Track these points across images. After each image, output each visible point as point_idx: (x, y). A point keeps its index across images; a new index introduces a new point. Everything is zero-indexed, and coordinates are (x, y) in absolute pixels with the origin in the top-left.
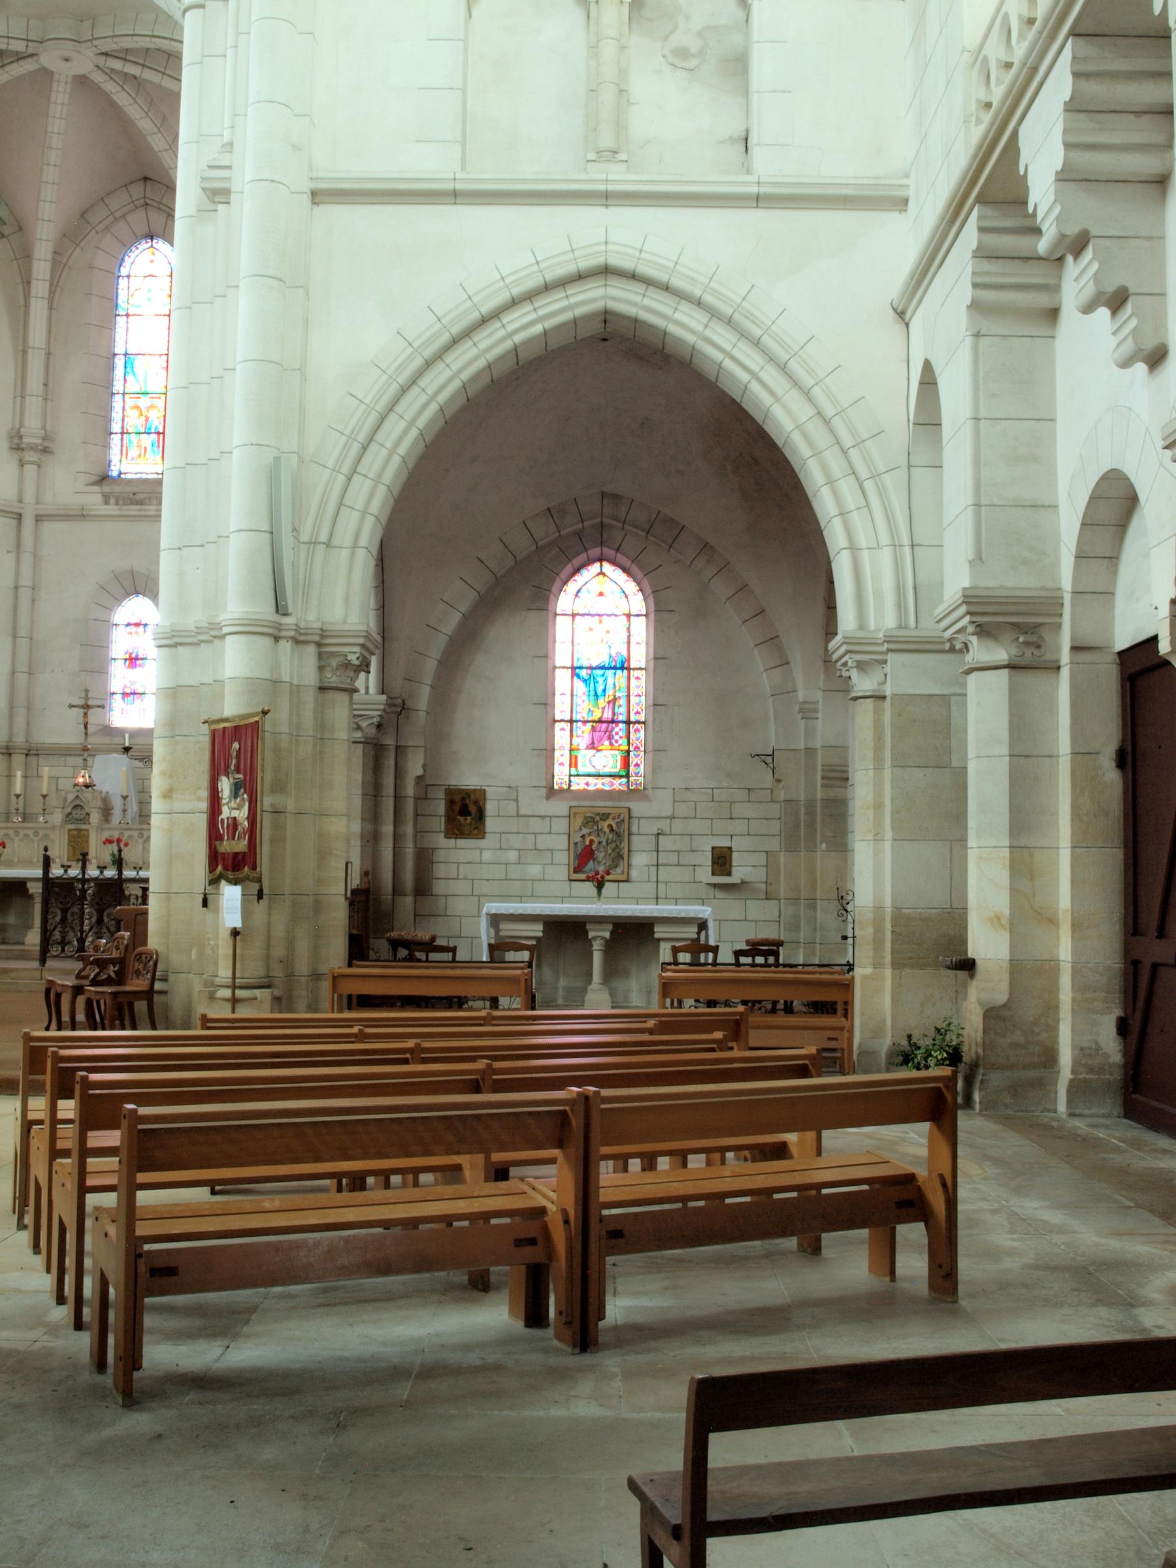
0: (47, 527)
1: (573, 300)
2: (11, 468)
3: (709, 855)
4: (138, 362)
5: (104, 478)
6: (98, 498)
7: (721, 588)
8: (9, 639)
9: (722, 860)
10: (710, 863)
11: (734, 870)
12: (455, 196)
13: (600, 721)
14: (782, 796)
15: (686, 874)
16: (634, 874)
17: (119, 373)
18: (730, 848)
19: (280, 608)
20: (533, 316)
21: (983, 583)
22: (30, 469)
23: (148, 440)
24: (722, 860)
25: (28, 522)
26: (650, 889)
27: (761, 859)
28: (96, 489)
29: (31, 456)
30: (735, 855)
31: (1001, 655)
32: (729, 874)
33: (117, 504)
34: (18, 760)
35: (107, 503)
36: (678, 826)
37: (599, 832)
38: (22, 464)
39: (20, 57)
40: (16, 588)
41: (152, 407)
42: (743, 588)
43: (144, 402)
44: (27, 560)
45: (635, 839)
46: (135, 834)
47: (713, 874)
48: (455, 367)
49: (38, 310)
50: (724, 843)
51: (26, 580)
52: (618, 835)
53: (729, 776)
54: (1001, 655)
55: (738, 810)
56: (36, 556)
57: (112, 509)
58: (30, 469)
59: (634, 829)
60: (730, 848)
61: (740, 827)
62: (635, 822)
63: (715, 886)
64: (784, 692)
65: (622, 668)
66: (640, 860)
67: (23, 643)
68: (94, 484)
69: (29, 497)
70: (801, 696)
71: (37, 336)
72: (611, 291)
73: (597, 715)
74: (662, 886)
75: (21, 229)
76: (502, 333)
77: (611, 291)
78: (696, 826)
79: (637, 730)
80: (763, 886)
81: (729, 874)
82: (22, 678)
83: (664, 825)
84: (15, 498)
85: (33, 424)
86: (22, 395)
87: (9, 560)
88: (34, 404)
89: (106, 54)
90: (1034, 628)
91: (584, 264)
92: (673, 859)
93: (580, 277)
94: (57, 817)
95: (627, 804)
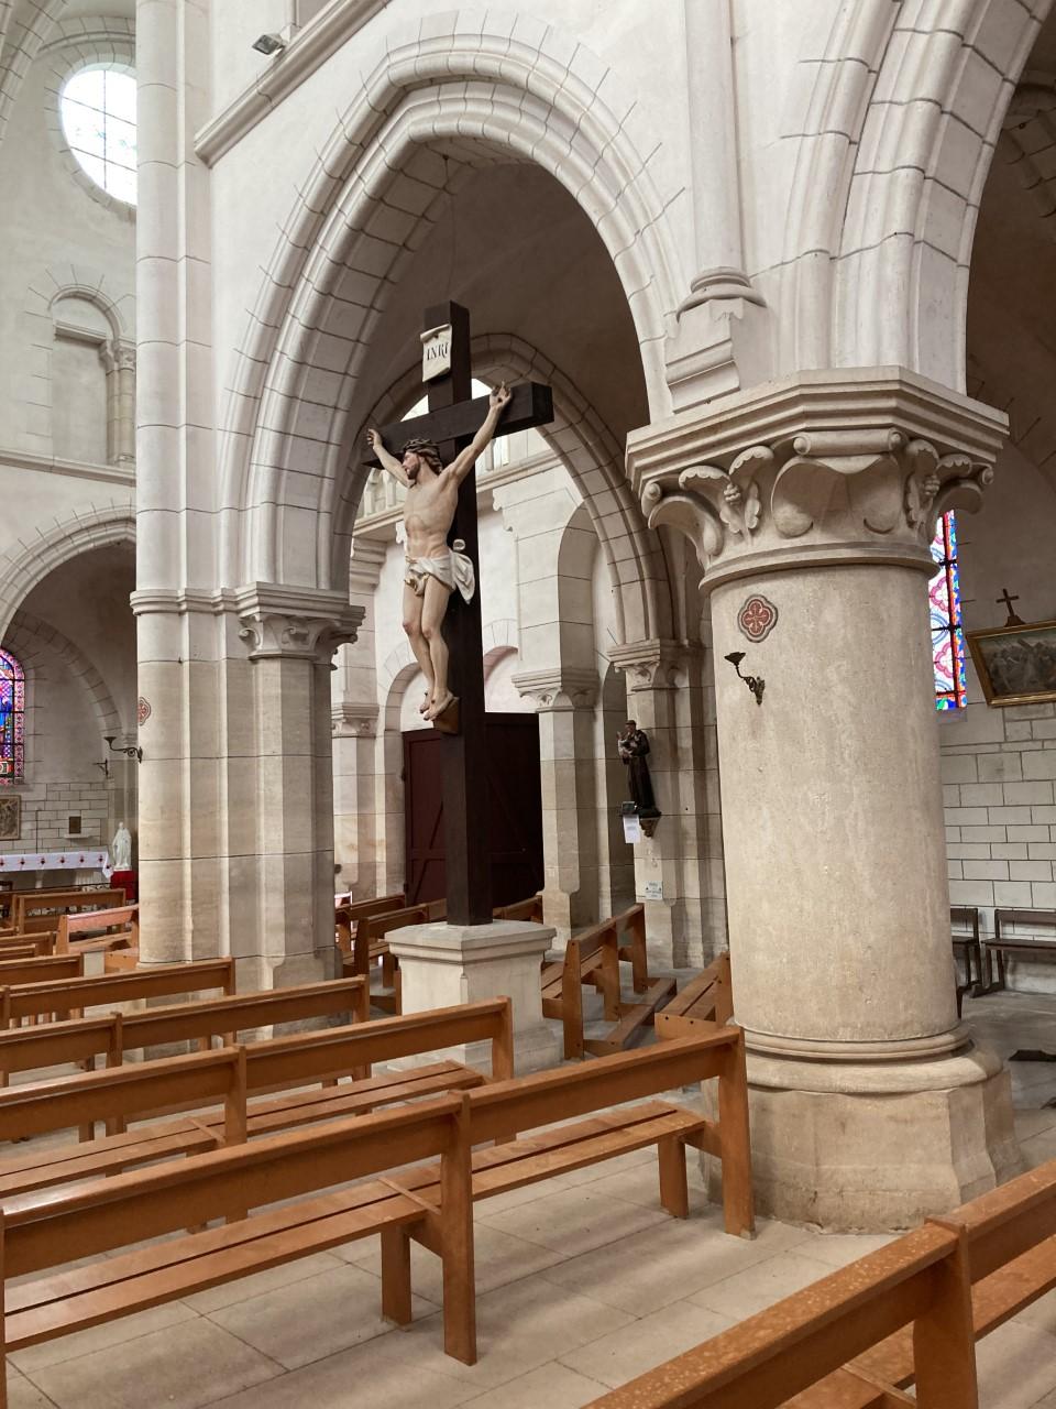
1: (109, 532)
3: (68, 821)
7: (75, 670)
9: (75, 825)
11: (82, 830)
12: (51, 469)
15: (53, 833)
16: (23, 835)
18: (80, 818)
20: (88, 538)
21: (350, 701)
24: (75, 825)
26: (32, 844)
27: (98, 823)
30: (82, 822)
31: (353, 731)
32: (80, 832)
36: (49, 806)
45: (23, 814)
47: (70, 833)
48: (46, 561)
50: (76, 814)
52: (13, 812)
53: (78, 776)
54: (353, 731)
60: (80, 818)
61: (85, 805)
62: (23, 804)
63: (71, 839)
65: (10, 712)
66: (26, 827)
74: (40, 842)
78: (61, 805)
79: (19, 749)
80: (98, 838)
81: (80, 832)
83: (41, 805)
90: (366, 721)
95: (17, 793)
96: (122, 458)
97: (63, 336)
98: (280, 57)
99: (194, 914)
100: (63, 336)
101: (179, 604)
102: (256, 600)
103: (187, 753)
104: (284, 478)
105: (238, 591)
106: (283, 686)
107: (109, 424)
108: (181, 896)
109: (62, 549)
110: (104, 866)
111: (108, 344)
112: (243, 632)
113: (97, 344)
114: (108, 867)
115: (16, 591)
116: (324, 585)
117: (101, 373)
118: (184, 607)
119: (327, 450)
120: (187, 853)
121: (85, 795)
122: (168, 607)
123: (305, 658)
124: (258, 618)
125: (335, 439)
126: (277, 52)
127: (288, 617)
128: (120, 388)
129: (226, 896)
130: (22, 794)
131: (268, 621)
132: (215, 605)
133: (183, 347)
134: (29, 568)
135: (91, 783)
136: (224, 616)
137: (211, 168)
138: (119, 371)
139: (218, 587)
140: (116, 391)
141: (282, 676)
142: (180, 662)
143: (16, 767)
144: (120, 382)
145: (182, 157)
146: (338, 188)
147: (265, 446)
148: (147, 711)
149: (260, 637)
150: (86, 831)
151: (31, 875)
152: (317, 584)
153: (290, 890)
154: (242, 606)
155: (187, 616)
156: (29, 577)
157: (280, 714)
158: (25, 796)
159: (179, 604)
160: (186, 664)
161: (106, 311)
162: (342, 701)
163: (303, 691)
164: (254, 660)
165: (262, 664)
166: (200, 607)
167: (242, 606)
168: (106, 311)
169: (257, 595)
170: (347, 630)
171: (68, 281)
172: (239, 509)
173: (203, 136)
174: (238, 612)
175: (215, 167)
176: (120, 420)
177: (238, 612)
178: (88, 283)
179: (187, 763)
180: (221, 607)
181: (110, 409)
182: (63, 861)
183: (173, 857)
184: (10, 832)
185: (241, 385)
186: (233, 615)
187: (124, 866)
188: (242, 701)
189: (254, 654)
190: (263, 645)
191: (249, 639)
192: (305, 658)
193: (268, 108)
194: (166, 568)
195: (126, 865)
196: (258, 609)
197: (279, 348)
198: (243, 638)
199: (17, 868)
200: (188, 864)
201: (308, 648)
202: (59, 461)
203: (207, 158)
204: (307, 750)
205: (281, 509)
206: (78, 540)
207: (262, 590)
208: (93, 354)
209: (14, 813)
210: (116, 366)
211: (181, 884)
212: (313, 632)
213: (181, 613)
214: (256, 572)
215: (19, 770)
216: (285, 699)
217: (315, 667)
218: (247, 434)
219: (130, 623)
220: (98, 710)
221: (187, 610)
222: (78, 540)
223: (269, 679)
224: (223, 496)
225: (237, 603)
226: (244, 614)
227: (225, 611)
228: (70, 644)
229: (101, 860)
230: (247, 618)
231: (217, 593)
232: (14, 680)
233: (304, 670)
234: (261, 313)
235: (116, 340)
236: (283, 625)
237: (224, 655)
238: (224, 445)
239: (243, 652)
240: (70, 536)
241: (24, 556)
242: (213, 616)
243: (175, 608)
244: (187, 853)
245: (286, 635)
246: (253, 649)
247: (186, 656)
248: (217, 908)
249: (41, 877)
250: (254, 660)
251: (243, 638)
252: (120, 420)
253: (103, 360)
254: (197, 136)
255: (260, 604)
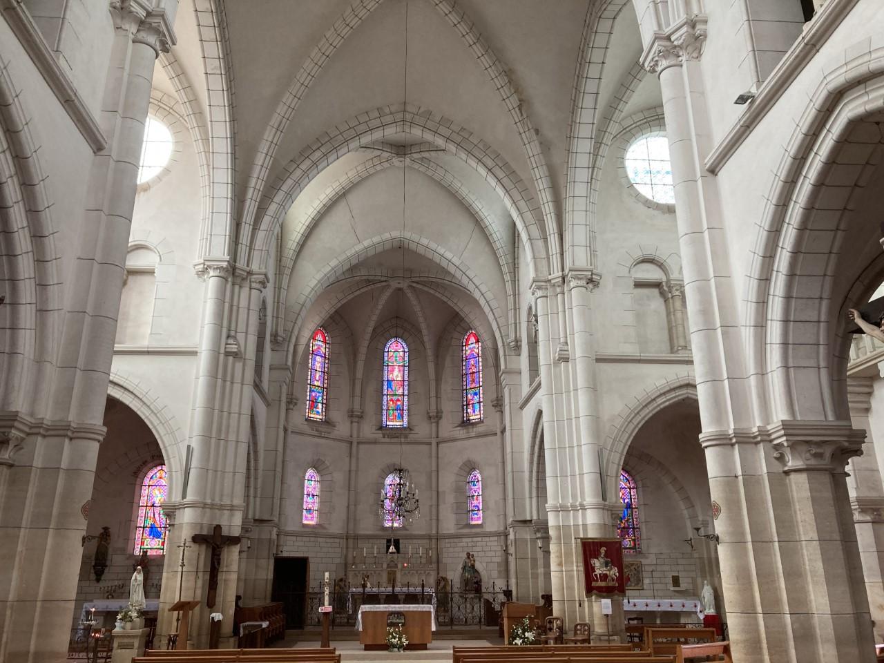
0: (361, 446)
1: (677, 394)
2: (348, 424)
4: (393, 383)
5: (381, 428)
6: (381, 435)
8: (347, 492)
9: (676, 581)
10: (671, 582)
11: (681, 585)
12: (639, 361)
13: (624, 528)
14: (696, 555)
16: (645, 587)
17: (385, 387)
18: (678, 577)
19: (604, 499)
20: (665, 399)
21: (861, 495)
22: (355, 424)
23: (396, 413)
24: (676, 581)
25: (355, 444)
27: (690, 580)
28: (380, 432)
29: (356, 420)
32: (679, 586)
33: (388, 438)
34: (351, 541)
35: (384, 437)
36: (659, 568)
37: (631, 571)
38: (352, 422)
39: (380, 282)
40: (350, 471)
41: (398, 400)
42: (675, 479)
43: (395, 398)
44: (354, 460)
46: (415, 572)
48: (642, 416)
49: (360, 366)
51: (353, 468)
54: (868, 518)
55: (680, 561)
56: (357, 459)
57: (387, 440)
58: (355, 424)
59: (643, 569)
61: (681, 568)
64: (693, 517)
65: (630, 508)
66: (646, 581)
67: (352, 493)
68: (378, 430)
69: (355, 435)
70: (700, 518)
71: (359, 374)
72: (689, 391)
73: (623, 525)
75: (352, 334)
76: (656, 405)
77: (689, 391)
78: (666, 568)
81: (679, 586)
82: (352, 507)
83: (653, 567)
84: (349, 434)
85: (357, 407)
86: (353, 395)
87: (347, 460)
88: (357, 400)
89: (413, 282)
90: (877, 510)
91: (682, 383)
92: (658, 581)
93: (680, 387)
94: (385, 566)
95: (638, 560)
96: (680, 348)
97: (639, 285)
98: (752, 102)
99: (770, 654)
100: (639, 285)
101: (731, 439)
102: (782, 432)
103: (749, 538)
104: (790, 352)
105: (769, 427)
106: (811, 490)
107: (670, 330)
108: (759, 641)
109: (651, 407)
110: (699, 611)
111: (664, 284)
112: (776, 454)
113: (657, 285)
114: (701, 612)
115: (627, 435)
116: (831, 417)
117: (661, 301)
118: (734, 440)
119: (819, 327)
120: (759, 609)
121: (680, 561)
122: (723, 441)
123: (826, 470)
124: (785, 444)
125: (823, 318)
126: (749, 101)
127: (807, 442)
128: (674, 308)
129: (792, 643)
130: (642, 560)
131: (793, 446)
132: (755, 437)
133: (713, 281)
134: (633, 421)
135: (683, 554)
136: (762, 444)
137: (716, 175)
138: (672, 298)
139: (755, 426)
140: (672, 310)
141: (809, 483)
142: (736, 477)
143: (637, 543)
144: (673, 303)
145: (699, 174)
146: (802, 163)
147: (774, 331)
148: (718, 510)
149: (789, 457)
150: (684, 585)
151: (652, 614)
152: (826, 417)
153: (840, 642)
154: (773, 436)
155: (737, 446)
156: (633, 426)
157: (812, 511)
158: (644, 561)
159: (731, 439)
160: (741, 478)
161: (661, 265)
162: (856, 495)
163: (828, 494)
164: (787, 473)
165: (793, 476)
166: (745, 440)
167: (773, 436)
168: (661, 265)
169: (783, 429)
170: (854, 447)
171: (638, 254)
172: (762, 374)
173: (709, 160)
174: (771, 441)
175: (719, 174)
176: (676, 326)
177: (771, 441)
178: (649, 253)
179: (750, 546)
180: (759, 439)
181: (669, 321)
182: (671, 606)
183: (748, 610)
184: (637, 584)
185: (753, 296)
186: (768, 444)
187: (711, 611)
188: (783, 502)
189: (786, 469)
190: (791, 463)
191: (781, 459)
192: (826, 470)
193: (748, 132)
194: (719, 417)
195: (713, 611)
196: (784, 438)
197: (775, 269)
198: (777, 459)
199: (644, 609)
200: (760, 617)
201: (826, 462)
202: (644, 356)
203: (713, 171)
204: (837, 536)
205: (792, 370)
206: (660, 401)
207: (785, 425)
208: (656, 291)
209: (638, 572)
210: (670, 295)
211: (757, 631)
212: (828, 451)
213: (733, 445)
214: (780, 414)
215: (639, 545)
216: (814, 500)
217: (833, 475)
218: (761, 325)
219: (700, 453)
220: (682, 505)
221: (736, 442)
222: (660, 401)
223: (800, 487)
224: (750, 366)
225: (770, 435)
226: (775, 442)
227: (762, 441)
228: (660, 464)
229: (696, 606)
230: (778, 444)
231: (755, 430)
232: (630, 488)
233: (826, 479)
234: (760, 250)
235: (668, 281)
236: (804, 448)
237: (765, 470)
238: (747, 336)
239: (779, 468)
240: (654, 399)
241: (630, 414)
242: (753, 445)
243: (728, 441)
244: (759, 609)
245: (808, 454)
246: (785, 465)
247: (739, 473)
248: (786, 651)
249: (659, 615)
250: (787, 473)
251: (777, 459)
252: (676, 326)
253: (662, 294)
254: (706, 161)
255: (785, 435)
